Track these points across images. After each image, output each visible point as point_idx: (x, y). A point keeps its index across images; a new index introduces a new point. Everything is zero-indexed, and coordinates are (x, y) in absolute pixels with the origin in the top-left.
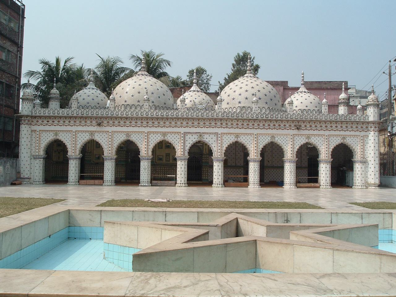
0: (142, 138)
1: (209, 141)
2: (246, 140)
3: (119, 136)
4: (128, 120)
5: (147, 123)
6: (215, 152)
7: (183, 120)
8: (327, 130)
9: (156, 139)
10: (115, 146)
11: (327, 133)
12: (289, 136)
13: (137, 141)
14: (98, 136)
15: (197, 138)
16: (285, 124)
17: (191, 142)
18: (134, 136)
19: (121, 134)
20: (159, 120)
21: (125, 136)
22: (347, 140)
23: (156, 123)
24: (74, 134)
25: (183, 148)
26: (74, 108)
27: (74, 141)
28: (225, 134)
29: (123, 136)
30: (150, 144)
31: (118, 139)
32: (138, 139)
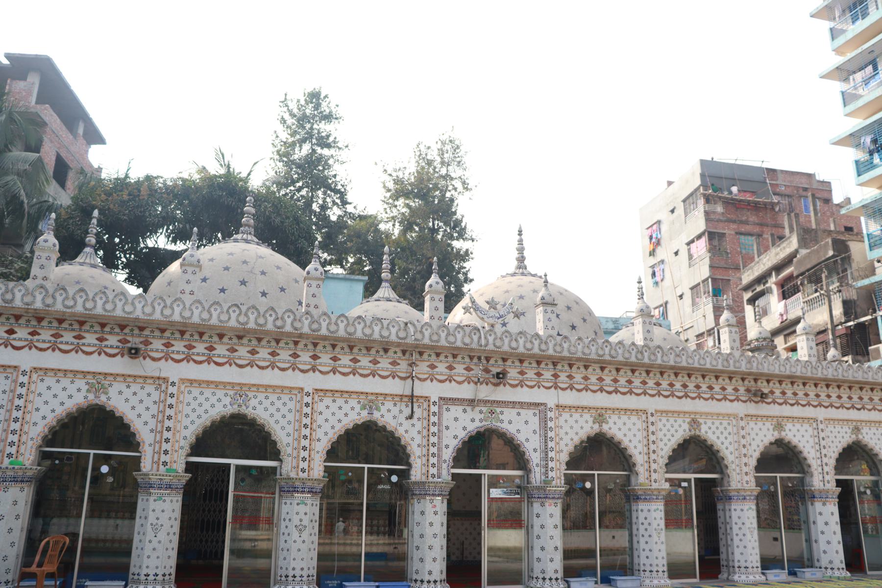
0: (290, 411)
1: (518, 431)
2: (625, 430)
3: (207, 399)
4: (245, 341)
5: (315, 357)
6: (537, 469)
7: (438, 355)
9: (342, 417)
10: (185, 438)
11: (821, 413)
12: (734, 422)
13: (272, 421)
14: (124, 396)
15: (481, 421)
16: (724, 383)
17: (462, 435)
18: (261, 403)
19: (214, 394)
20: (355, 350)
21: (227, 401)
22: (864, 435)
23: (345, 360)
24: (25, 379)
25: (436, 452)
26: (39, 281)
27: (18, 408)
28: (567, 410)
29: (219, 400)
30: (320, 434)
31: (200, 411)
32: (278, 416)
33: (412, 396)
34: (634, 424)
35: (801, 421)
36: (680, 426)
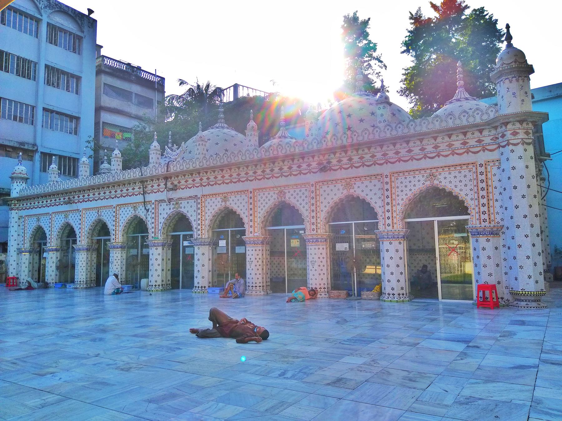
8: (387, 162)
28: (208, 197)
33: (144, 202)
34: (243, 199)
35: (368, 178)
36: (272, 196)
